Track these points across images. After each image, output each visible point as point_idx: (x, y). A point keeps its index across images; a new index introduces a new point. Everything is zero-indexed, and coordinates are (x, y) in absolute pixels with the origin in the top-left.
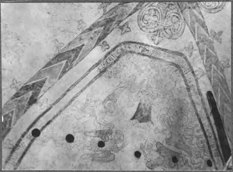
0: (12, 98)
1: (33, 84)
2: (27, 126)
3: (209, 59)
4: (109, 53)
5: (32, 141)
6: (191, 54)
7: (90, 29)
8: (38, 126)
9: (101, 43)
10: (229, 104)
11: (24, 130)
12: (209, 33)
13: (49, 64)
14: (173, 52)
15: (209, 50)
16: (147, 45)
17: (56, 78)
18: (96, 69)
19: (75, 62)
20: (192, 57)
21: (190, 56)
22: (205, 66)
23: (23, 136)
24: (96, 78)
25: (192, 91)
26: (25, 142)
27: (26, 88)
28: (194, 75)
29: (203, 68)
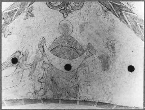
3: (8, 16)
12: (30, 6)
15: (16, 13)
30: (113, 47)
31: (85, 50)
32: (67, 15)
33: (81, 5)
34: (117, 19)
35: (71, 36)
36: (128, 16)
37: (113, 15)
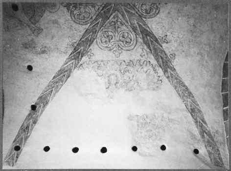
30: (44, 52)
31: (36, 25)
32: (65, 6)
33: (76, 21)
34: (67, 56)
35: (45, 10)
36: (71, 65)
37: (71, 52)
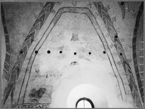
0: (25, 41)
1: (31, 34)
2: (33, 50)
4: (56, 15)
5: (36, 55)
6: (91, 7)
7: (46, 6)
8: (36, 50)
9: (52, 11)
10: (112, 26)
11: (32, 52)
13: (35, 24)
14: (83, 8)
16: (70, 7)
17: (38, 30)
18: (53, 23)
19: (44, 22)
20: (92, 8)
21: (91, 8)
22: (99, 11)
23: (32, 54)
24: (54, 26)
25: (94, 24)
26: (33, 56)
27: (29, 36)
28: (94, 16)
29: (98, 12)
